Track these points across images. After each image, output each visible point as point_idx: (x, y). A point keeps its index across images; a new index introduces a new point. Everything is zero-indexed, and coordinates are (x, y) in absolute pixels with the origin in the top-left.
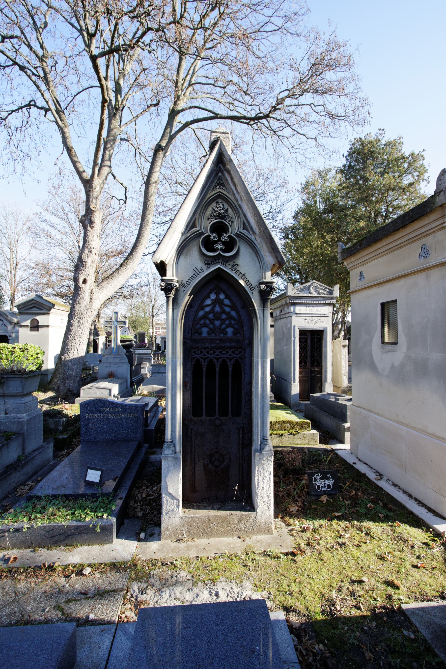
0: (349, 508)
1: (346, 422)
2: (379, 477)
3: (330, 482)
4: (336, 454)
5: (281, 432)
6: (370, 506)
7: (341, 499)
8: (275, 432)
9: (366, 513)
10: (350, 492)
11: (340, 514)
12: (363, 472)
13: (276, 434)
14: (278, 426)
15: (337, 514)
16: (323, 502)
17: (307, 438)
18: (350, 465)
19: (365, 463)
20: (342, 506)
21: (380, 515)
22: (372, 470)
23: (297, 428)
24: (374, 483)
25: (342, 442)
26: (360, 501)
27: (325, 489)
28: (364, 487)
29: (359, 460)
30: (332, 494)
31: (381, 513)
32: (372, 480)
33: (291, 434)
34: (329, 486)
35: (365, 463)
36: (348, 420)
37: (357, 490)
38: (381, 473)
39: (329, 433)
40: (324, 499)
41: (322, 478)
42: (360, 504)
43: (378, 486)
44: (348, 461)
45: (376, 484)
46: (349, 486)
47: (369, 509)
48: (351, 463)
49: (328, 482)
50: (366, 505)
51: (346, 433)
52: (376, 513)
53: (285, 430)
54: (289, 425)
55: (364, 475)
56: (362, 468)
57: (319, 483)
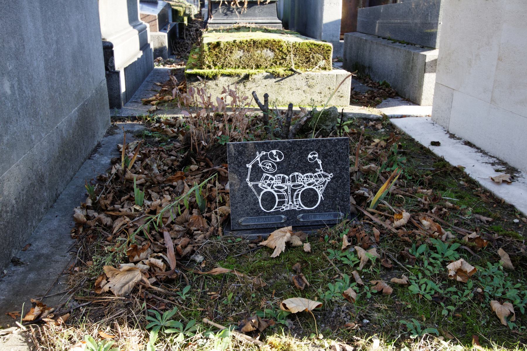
0: (367, 278)
1: (433, 48)
2: (507, 177)
3: (317, 181)
4: (392, 126)
5: (243, 72)
6: (459, 271)
7: (346, 243)
8: (227, 71)
9: (437, 299)
10: (390, 217)
11: (313, 305)
12: (454, 163)
13: (230, 75)
14: (238, 54)
15: (296, 305)
16: (272, 250)
17: (317, 89)
18: (422, 147)
19: (468, 144)
20: (343, 267)
21: (496, 305)
22: (486, 159)
23: (292, 60)
24: (486, 191)
25: (415, 101)
26: (423, 248)
27: (295, 204)
28: (449, 199)
29: (452, 136)
30: (320, 225)
31: (501, 300)
32: (482, 182)
33: (273, 75)
34: (309, 197)
35: (468, 144)
36: (438, 45)
37: (418, 210)
38: (512, 164)
39: (387, 86)
40: (279, 240)
41: (284, 168)
42: (419, 261)
43: (499, 202)
44: (417, 139)
45: (491, 195)
46: (391, 197)
47: (452, 282)
48: (426, 144)
49: (305, 181)
50: (444, 264)
51: (427, 75)
52: (479, 298)
53: (258, 67)
54: (271, 54)
55: (459, 171)
56: (453, 154)
57: (272, 183)
